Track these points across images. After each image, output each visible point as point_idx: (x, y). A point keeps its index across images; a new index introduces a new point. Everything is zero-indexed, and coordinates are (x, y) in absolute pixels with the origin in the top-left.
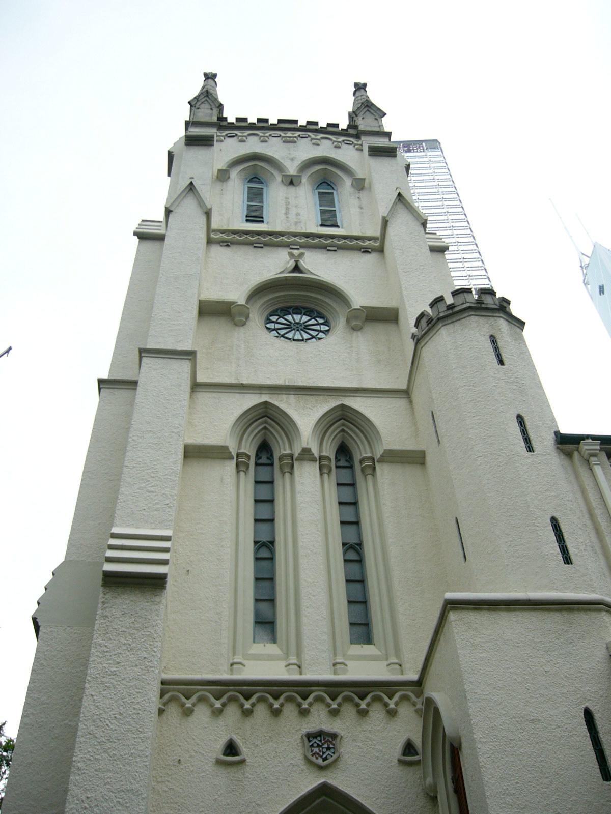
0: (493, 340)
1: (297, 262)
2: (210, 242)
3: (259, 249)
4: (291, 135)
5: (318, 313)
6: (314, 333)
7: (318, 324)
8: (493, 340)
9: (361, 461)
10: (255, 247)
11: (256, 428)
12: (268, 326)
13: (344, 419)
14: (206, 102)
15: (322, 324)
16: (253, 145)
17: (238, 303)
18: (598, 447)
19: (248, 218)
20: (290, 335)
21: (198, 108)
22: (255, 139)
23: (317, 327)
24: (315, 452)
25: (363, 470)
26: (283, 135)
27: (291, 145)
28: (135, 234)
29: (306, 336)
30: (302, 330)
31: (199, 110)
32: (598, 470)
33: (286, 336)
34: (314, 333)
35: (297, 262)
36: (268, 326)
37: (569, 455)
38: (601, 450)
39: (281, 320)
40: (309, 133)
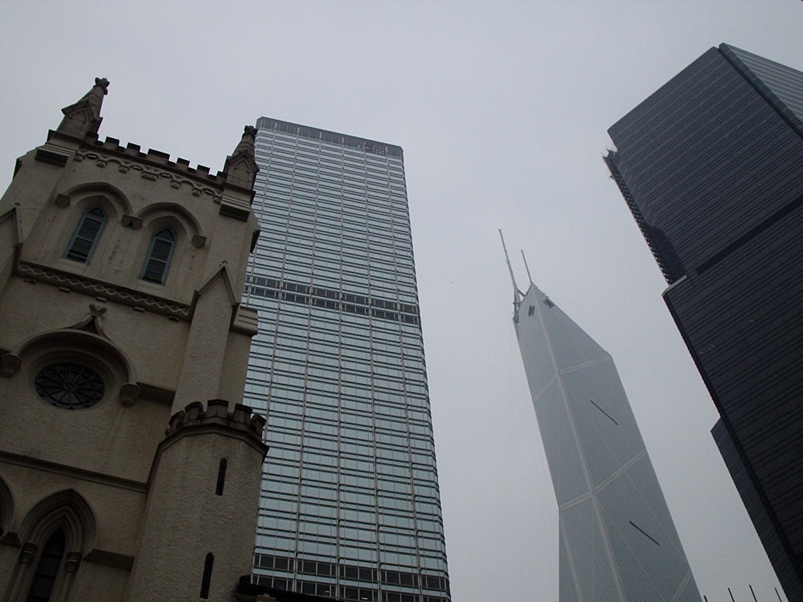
0: (223, 465)
1: (94, 318)
2: (15, 274)
3: (64, 294)
4: (153, 172)
8: (223, 465)
9: (69, 555)
10: (61, 290)
14: (82, 113)
16: (110, 175)
17: (11, 354)
19: (72, 254)
21: (71, 118)
22: (116, 166)
24: (22, 539)
25: (67, 565)
26: (145, 170)
27: (149, 182)
30: (72, 392)
31: (71, 120)
33: (52, 396)
35: (94, 318)
40: (171, 174)
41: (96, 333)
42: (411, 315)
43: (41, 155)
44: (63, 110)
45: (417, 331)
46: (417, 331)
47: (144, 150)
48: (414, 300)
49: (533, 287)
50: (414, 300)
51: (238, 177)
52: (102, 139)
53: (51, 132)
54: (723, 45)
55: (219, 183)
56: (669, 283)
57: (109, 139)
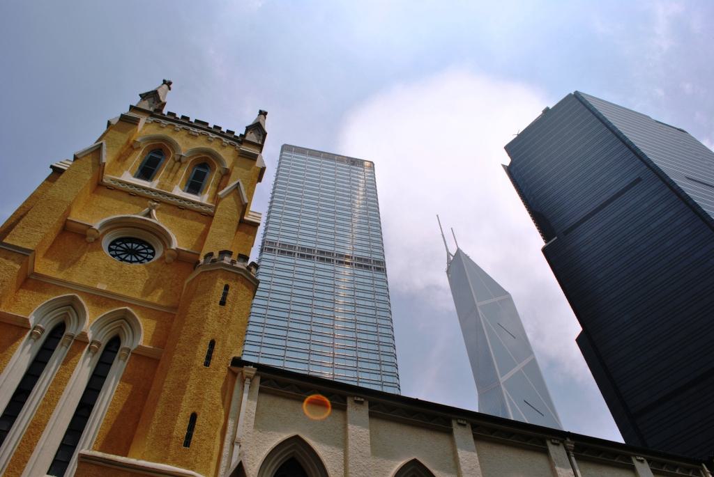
0: (227, 288)
5: (147, 244)
6: (140, 258)
7: (148, 253)
8: (227, 288)
11: (59, 312)
12: (112, 247)
13: (125, 319)
15: (150, 254)
18: (254, 372)
20: (128, 258)
23: (145, 255)
28: (52, 167)
29: (134, 259)
32: (247, 387)
34: (140, 258)
35: (150, 211)
36: (112, 247)
37: (235, 374)
38: (256, 375)
39: (124, 246)
41: (150, 217)
42: (380, 267)
43: (124, 118)
44: (140, 95)
45: (384, 277)
46: (384, 277)
47: (192, 120)
48: (382, 257)
49: (459, 251)
50: (382, 257)
51: (252, 137)
52: (165, 112)
53: (131, 107)
54: (576, 92)
55: (242, 140)
56: (546, 242)
57: (169, 113)
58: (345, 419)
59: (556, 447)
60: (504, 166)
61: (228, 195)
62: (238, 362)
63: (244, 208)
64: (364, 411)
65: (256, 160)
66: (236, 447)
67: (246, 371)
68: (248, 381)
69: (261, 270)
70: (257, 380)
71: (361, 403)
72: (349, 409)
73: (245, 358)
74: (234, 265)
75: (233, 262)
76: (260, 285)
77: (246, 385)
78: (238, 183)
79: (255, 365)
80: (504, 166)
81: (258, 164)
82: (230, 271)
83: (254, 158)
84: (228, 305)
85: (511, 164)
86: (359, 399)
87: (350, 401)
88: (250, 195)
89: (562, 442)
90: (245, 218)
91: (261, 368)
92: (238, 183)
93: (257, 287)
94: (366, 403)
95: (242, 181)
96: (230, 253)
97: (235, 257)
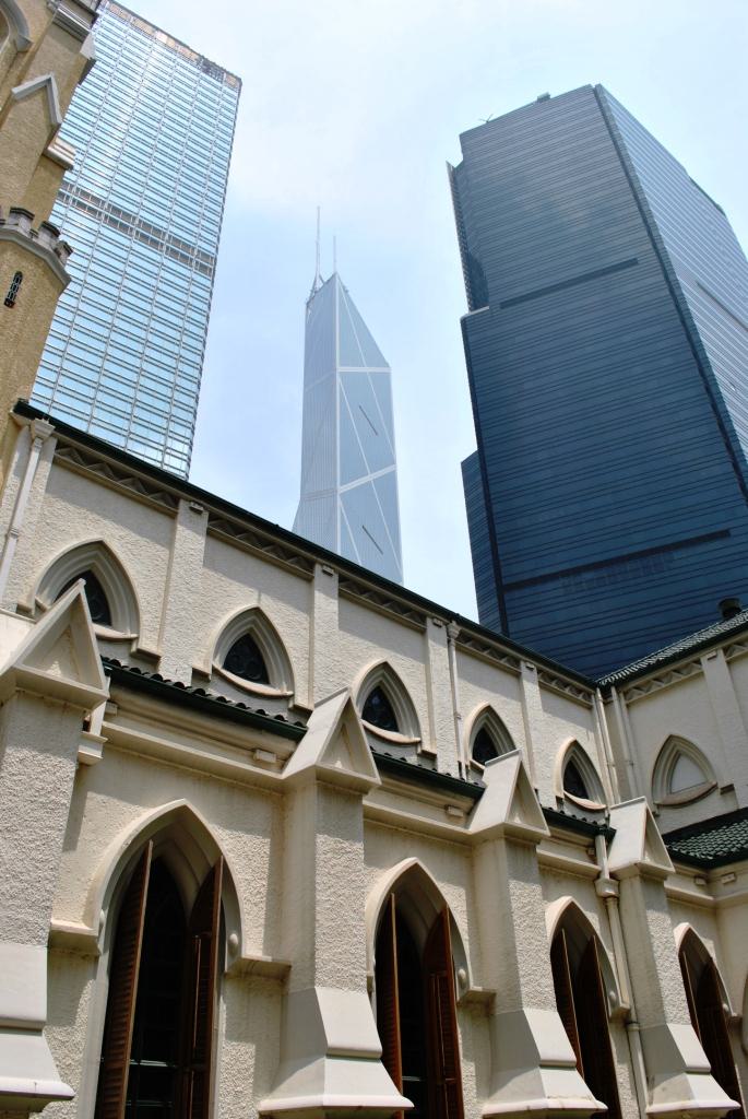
0: (19, 277)
8: (19, 277)
18: (50, 432)
32: (35, 455)
37: (18, 427)
38: (52, 435)
42: (207, 266)
50: (213, 250)
58: (173, 530)
59: (437, 628)
60: (449, 165)
61: (28, 95)
62: (23, 409)
63: (54, 130)
64: (203, 521)
65: (82, 42)
66: (12, 541)
67: (38, 427)
68: (38, 441)
69: (72, 257)
70: (53, 443)
71: (199, 512)
72: (180, 517)
73: (32, 404)
74: (34, 240)
75: (33, 233)
76: (71, 286)
77: (33, 448)
78: (49, 80)
79: (53, 421)
80: (449, 165)
81: (86, 50)
82: (24, 246)
83: (79, 36)
84: (19, 309)
85: (462, 165)
86: (197, 507)
87: (183, 506)
88: (65, 103)
89: (446, 625)
90: (50, 148)
91: (61, 427)
92: (49, 80)
93: (65, 287)
94: (206, 515)
95: (55, 77)
96: (30, 216)
97: (37, 224)
